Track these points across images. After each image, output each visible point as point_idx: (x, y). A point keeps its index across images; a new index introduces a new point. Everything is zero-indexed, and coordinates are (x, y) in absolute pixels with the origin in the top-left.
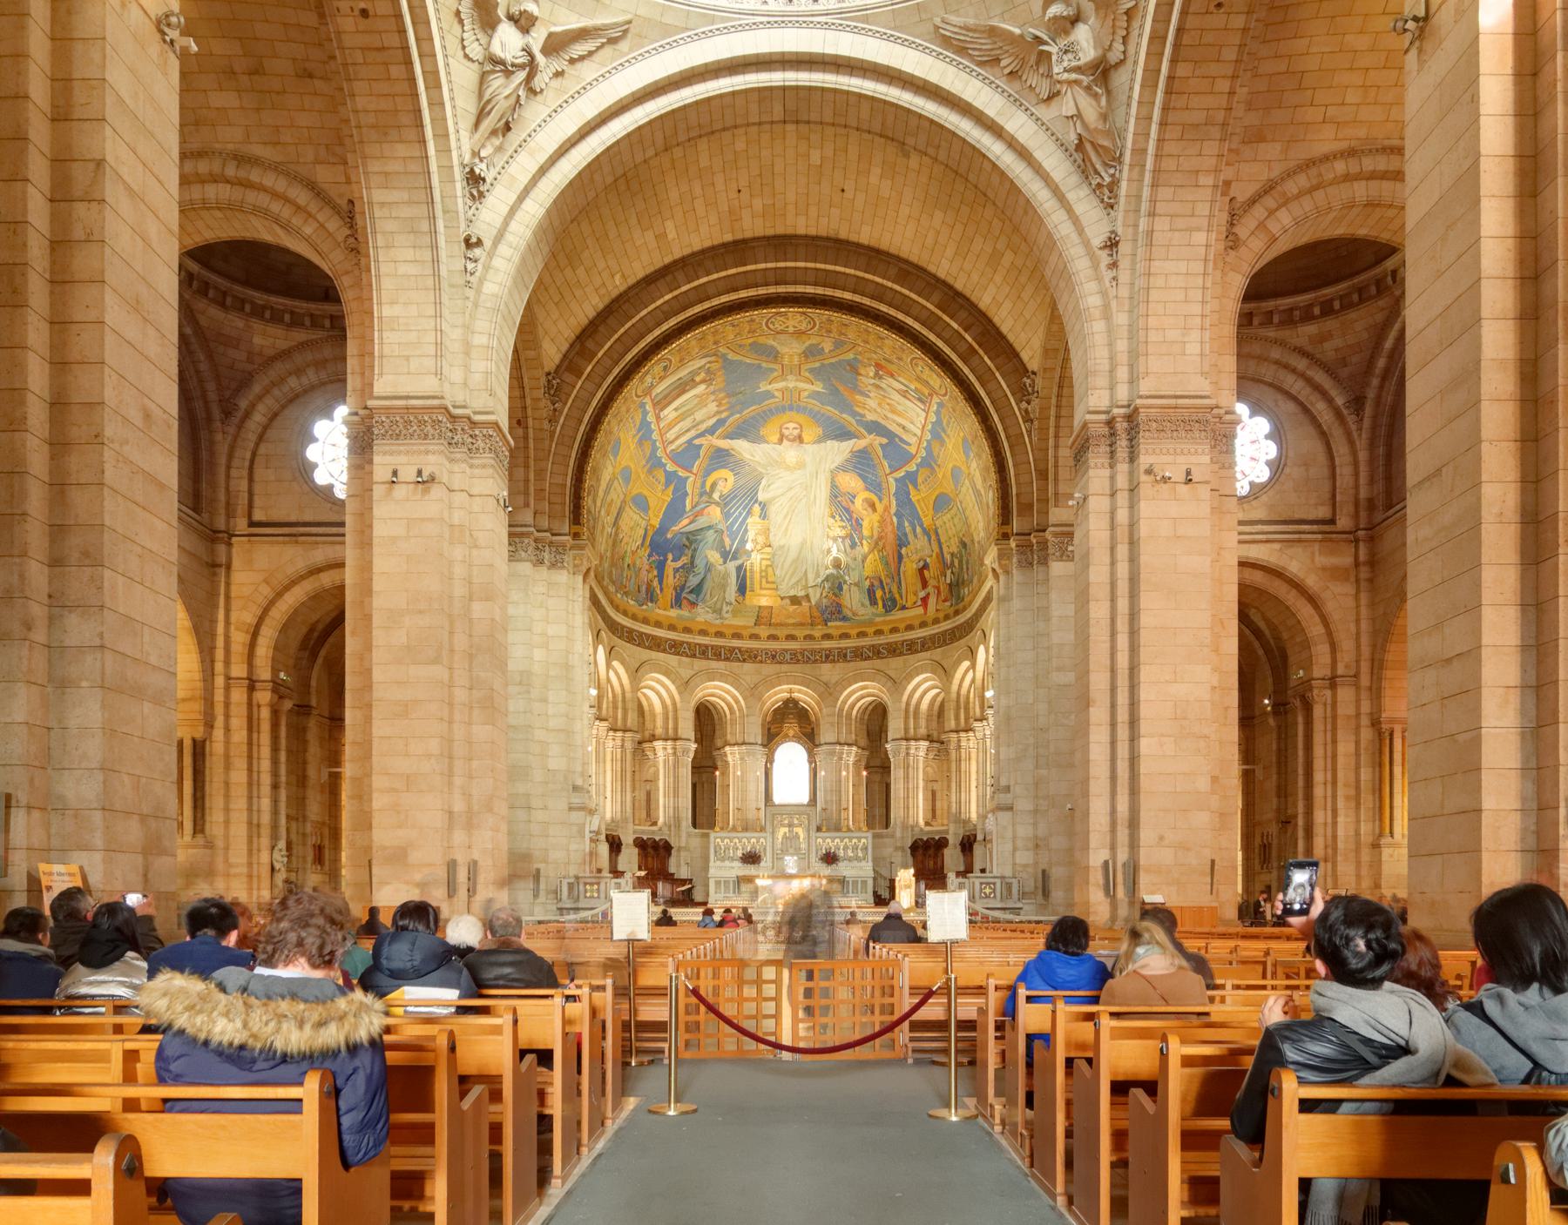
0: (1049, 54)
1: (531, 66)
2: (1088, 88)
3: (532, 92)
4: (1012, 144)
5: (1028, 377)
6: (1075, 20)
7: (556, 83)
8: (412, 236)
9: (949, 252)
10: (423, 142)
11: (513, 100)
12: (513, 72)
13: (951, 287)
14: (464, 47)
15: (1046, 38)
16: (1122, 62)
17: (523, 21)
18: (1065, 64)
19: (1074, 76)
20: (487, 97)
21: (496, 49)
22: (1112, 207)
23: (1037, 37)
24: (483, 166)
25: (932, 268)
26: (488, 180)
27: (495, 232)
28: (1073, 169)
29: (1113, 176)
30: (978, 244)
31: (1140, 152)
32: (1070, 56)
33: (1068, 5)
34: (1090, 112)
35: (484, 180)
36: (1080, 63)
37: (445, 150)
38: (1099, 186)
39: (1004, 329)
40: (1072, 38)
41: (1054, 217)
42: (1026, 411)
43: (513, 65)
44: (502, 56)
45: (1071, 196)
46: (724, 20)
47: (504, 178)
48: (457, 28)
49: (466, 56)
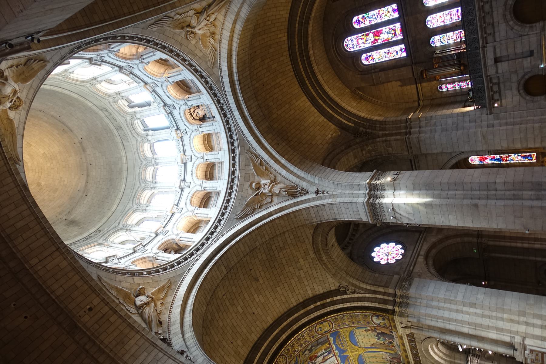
2: (276, 184)
4: (276, 212)
5: (340, 288)
6: (259, 183)
7: (163, 307)
9: (290, 296)
13: (301, 303)
15: (258, 192)
19: (271, 185)
23: (255, 195)
25: (292, 306)
30: (292, 281)
31: (298, 177)
38: (300, 193)
39: (322, 292)
42: (351, 292)
46: (191, 263)
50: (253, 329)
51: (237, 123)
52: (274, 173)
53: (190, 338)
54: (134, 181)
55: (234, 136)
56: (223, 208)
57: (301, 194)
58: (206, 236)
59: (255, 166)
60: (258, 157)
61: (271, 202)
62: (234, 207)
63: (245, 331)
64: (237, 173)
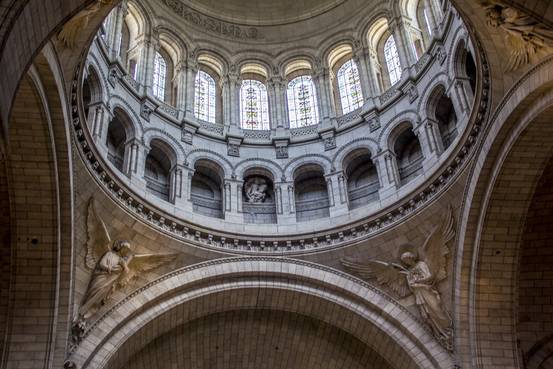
0: (406, 275)
1: (122, 271)
2: (429, 291)
3: (119, 287)
4: (388, 318)
6: (417, 260)
8: (32, 362)
10: (53, 308)
11: (108, 289)
12: (111, 275)
14: (85, 262)
15: (402, 267)
16: (445, 280)
17: (122, 251)
18: (416, 279)
19: (421, 285)
20: (94, 286)
21: (104, 263)
22: (452, 352)
24: (84, 323)
26: (85, 332)
27: (84, 361)
28: (425, 332)
29: (450, 335)
32: (417, 275)
33: (412, 253)
34: (433, 302)
35: (83, 331)
36: (424, 278)
37: (65, 313)
40: (417, 267)
41: (418, 357)
43: (112, 271)
44: (107, 266)
45: (427, 346)
47: (95, 331)
48: (83, 253)
49: (86, 266)
50: (259, 359)
51: (474, 165)
52: (450, 273)
53: (106, 353)
54: (358, 11)
55: (458, 171)
56: (344, 229)
57: (441, 344)
58: (286, 239)
59: (439, 234)
60: (455, 231)
61: (403, 298)
62: (355, 247)
63: (247, 351)
64: (409, 213)
